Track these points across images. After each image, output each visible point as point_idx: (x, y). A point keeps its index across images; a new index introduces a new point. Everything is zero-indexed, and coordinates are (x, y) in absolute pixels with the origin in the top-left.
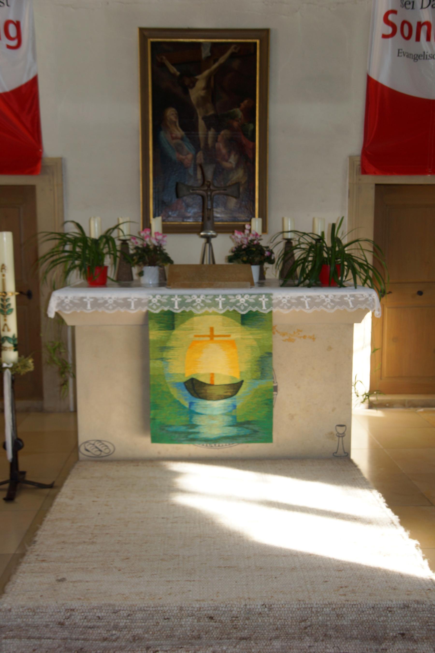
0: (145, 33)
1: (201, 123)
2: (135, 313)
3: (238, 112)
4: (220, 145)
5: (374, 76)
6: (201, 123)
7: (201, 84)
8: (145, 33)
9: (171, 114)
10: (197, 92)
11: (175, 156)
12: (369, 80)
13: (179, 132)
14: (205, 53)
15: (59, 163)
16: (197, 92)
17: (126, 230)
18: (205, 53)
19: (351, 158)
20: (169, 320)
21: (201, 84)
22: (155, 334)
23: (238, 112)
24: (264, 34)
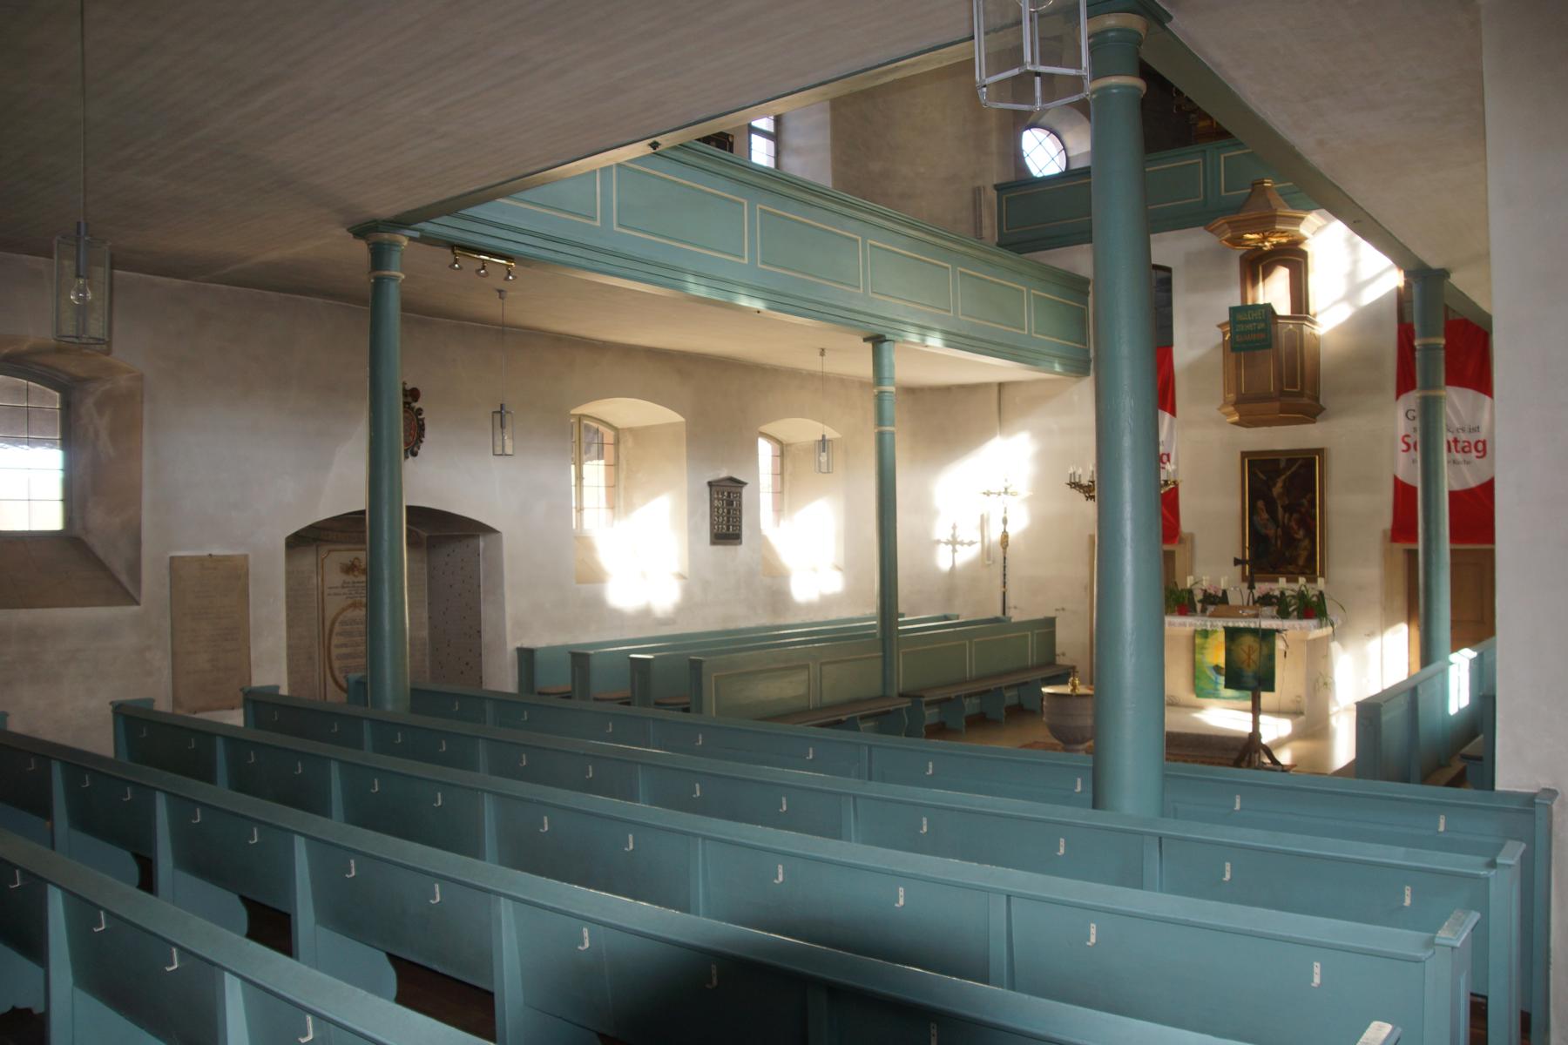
0: (1244, 455)
1: (1280, 510)
2: (1189, 630)
3: (1305, 502)
4: (1293, 524)
5: (1400, 477)
6: (1280, 510)
7: (1280, 484)
8: (1244, 455)
9: (1260, 504)
10: (1277, 489)
11: (1263, 531)
12: (1396, 480)
13: (1266, 516)
14: (1282, 465)
15: (1192, 536)
16: (1277, 489)
17: (1205, 585)
18: (1282, 465)
19: (1384, 532)
20: (1205, 634)
21: (1280, 484)
22: (1198, 641)
23: (1305, 502)
24: (1320, 452)
